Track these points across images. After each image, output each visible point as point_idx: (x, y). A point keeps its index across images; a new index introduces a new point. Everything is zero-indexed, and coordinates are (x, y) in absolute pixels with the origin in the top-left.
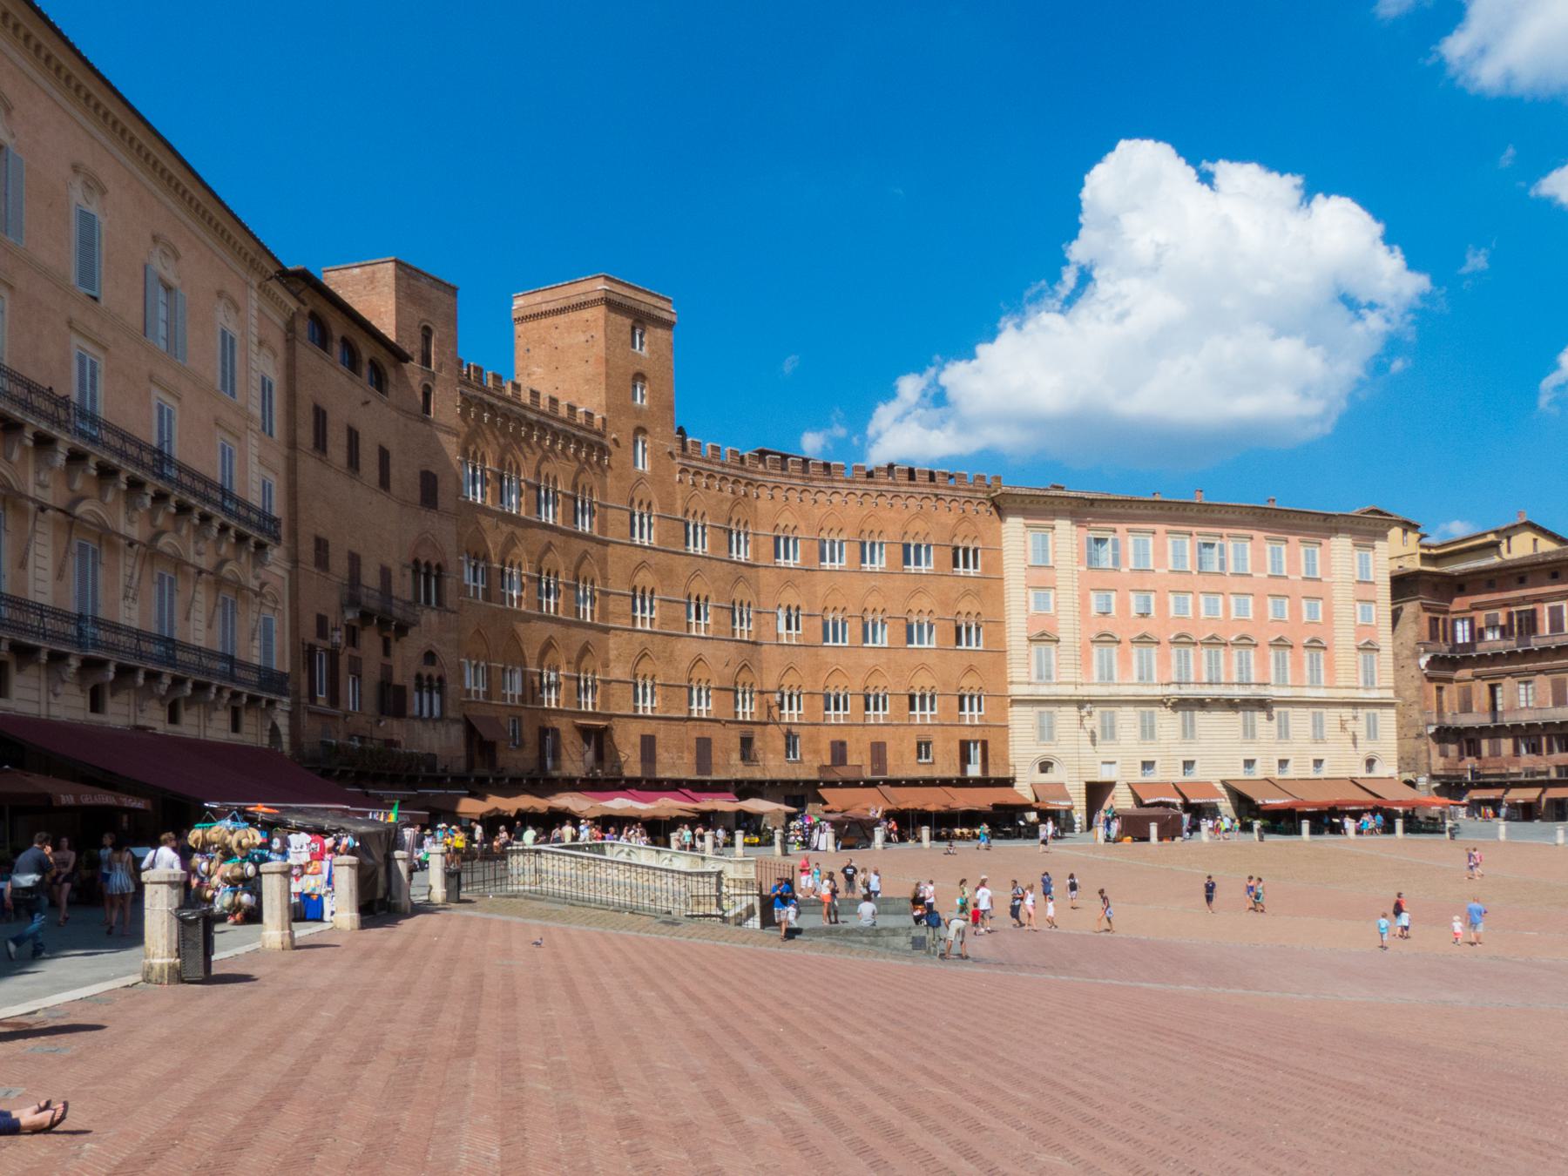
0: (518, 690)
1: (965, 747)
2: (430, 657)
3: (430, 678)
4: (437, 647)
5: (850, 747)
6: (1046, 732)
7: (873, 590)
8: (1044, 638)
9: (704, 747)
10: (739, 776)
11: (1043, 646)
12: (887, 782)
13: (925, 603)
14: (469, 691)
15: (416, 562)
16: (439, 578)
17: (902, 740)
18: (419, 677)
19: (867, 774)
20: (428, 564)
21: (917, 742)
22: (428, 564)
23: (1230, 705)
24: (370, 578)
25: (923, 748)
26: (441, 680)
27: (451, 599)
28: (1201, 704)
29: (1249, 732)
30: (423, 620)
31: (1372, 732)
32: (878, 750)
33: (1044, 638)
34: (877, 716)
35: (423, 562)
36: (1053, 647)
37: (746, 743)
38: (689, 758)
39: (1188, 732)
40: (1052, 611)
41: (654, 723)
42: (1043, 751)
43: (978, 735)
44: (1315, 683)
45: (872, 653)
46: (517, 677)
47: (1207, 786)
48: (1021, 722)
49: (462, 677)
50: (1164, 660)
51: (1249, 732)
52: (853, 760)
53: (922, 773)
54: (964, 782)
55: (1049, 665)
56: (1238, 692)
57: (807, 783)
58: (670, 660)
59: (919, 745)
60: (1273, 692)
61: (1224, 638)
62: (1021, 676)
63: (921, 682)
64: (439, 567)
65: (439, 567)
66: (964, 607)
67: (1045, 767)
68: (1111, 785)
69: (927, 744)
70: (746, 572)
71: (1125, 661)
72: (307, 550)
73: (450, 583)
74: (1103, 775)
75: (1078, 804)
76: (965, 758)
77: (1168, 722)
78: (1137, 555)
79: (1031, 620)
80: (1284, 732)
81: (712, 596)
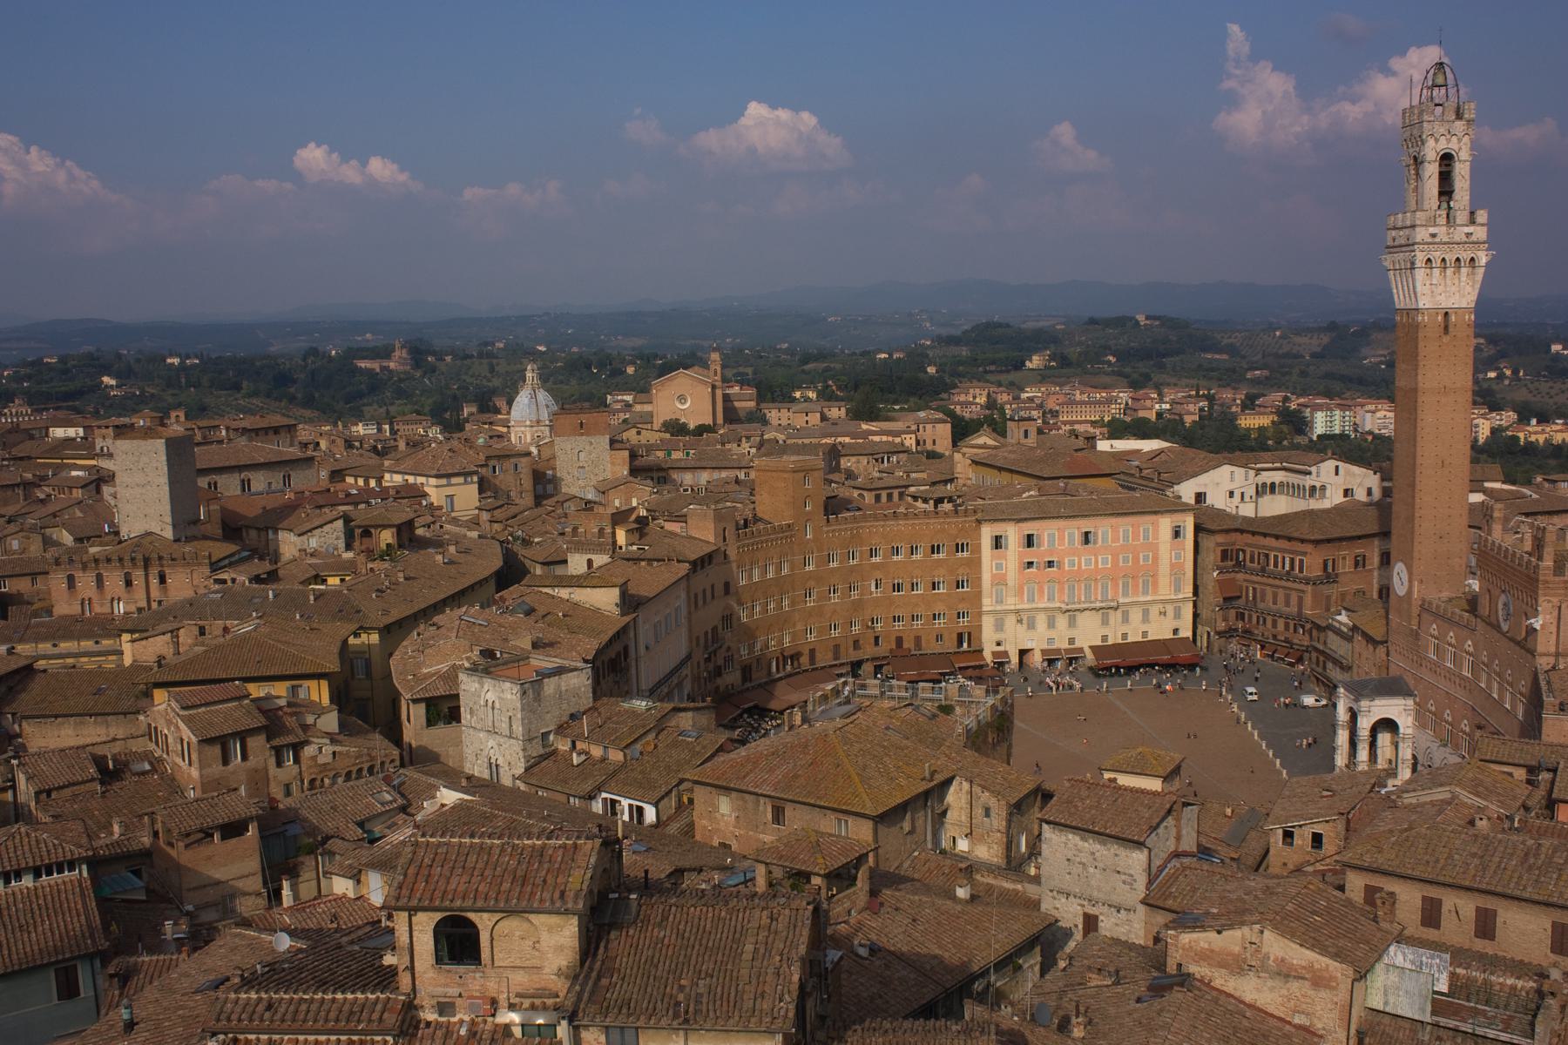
1: (960, 636)
6: (999, 626)
8: (999, 581)
13: (942, 571)
21: (935, 634)
25: (939, 637)
29: (1105, 622)
31: (1177, 615)
32: (918, 639)
34: (918, 624)
38: (830, 655)
39: (1072, 623)
42: (998, 637)
44: (1145, 593)
47: (1081, 650)
48: (987, 624)
50: (1061, 590)
51: (1105, 622)
52: (906, 645)
56: (1098, 605)
60: (1121, 600)
62: (987, 603)
63: (939, 608)
67: (998, 644)
71: (1041, 591)
75: (1015, 659)
76: (960, 643)
77: (1062, 621)
79: (993, 576)
80: (1126, 619)
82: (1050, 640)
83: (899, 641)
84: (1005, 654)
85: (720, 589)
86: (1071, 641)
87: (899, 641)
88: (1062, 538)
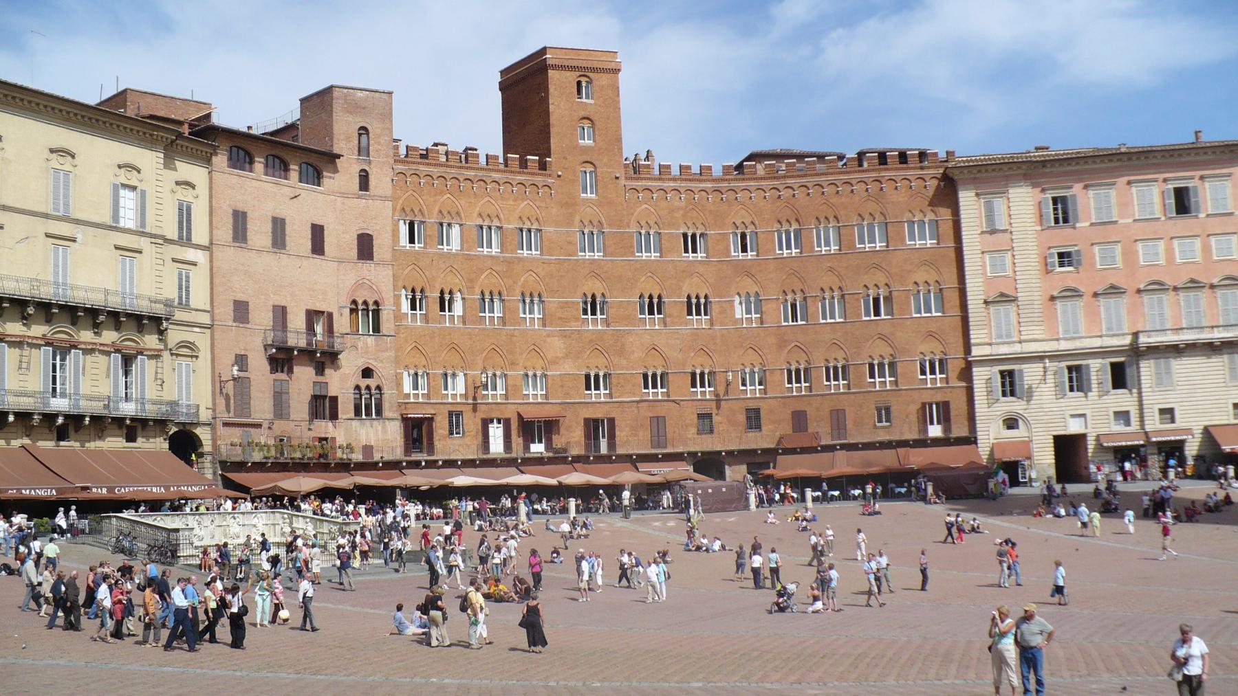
0: (461, 389)
2: (367, 373)
3: (368, 387)
4: (373, 364)
5: (811, 414)
7: (831, 269)
9: (658, 424)
10: (692, 449)
11: (1002, 308)
12: (844, 447)
13: (881, 278)
14: (409, 395)
15: (354, 302)
16: (377, 313)
17: (861, 407)
18: (358, 387)
19: (827, 441)
20: (365, 303)
22: (365, 303)
23: (1212, 348)
24: (297, 321)
25: (885, 413)
26: (378, 388)
27: (387, 325)
28: (1176, 350)
30: (360, 345)
33: (1006, 298)
35: (360, 302)
36: (1012, 308)
37: (705, 417)
38: (645, 435)
40: (1010, 273)
41: (606, 408)
43: (940, 397)
45: (828, 328)
46: (460, 380)
47: (1188, 431)
49: (399, 384)
53: (883, 437)
54: (923, 443)
55: (1009, 324)
57: (766, 451)
58: (621, 352)
59: (879, 410)
61: (1204, 279)
64: (376, 303)
65: (376, 303)
66: (920, 276)
67: (1011, 423)
68: (1081, 438)
69: (888, 410)
70: (702, 269)
72: (226, 312)
73: (386, 315)
74: (1074, 427)
76: (924, 419)
78: (1098, 209)
79: (988, 281)
81: (664, 294)
82: (1123, 416)
83: (799, 420)
84: (1027, 444)
85: (340, 240)
86: (1168, 413)
87: (799, 420)
88: (1124, 205)
